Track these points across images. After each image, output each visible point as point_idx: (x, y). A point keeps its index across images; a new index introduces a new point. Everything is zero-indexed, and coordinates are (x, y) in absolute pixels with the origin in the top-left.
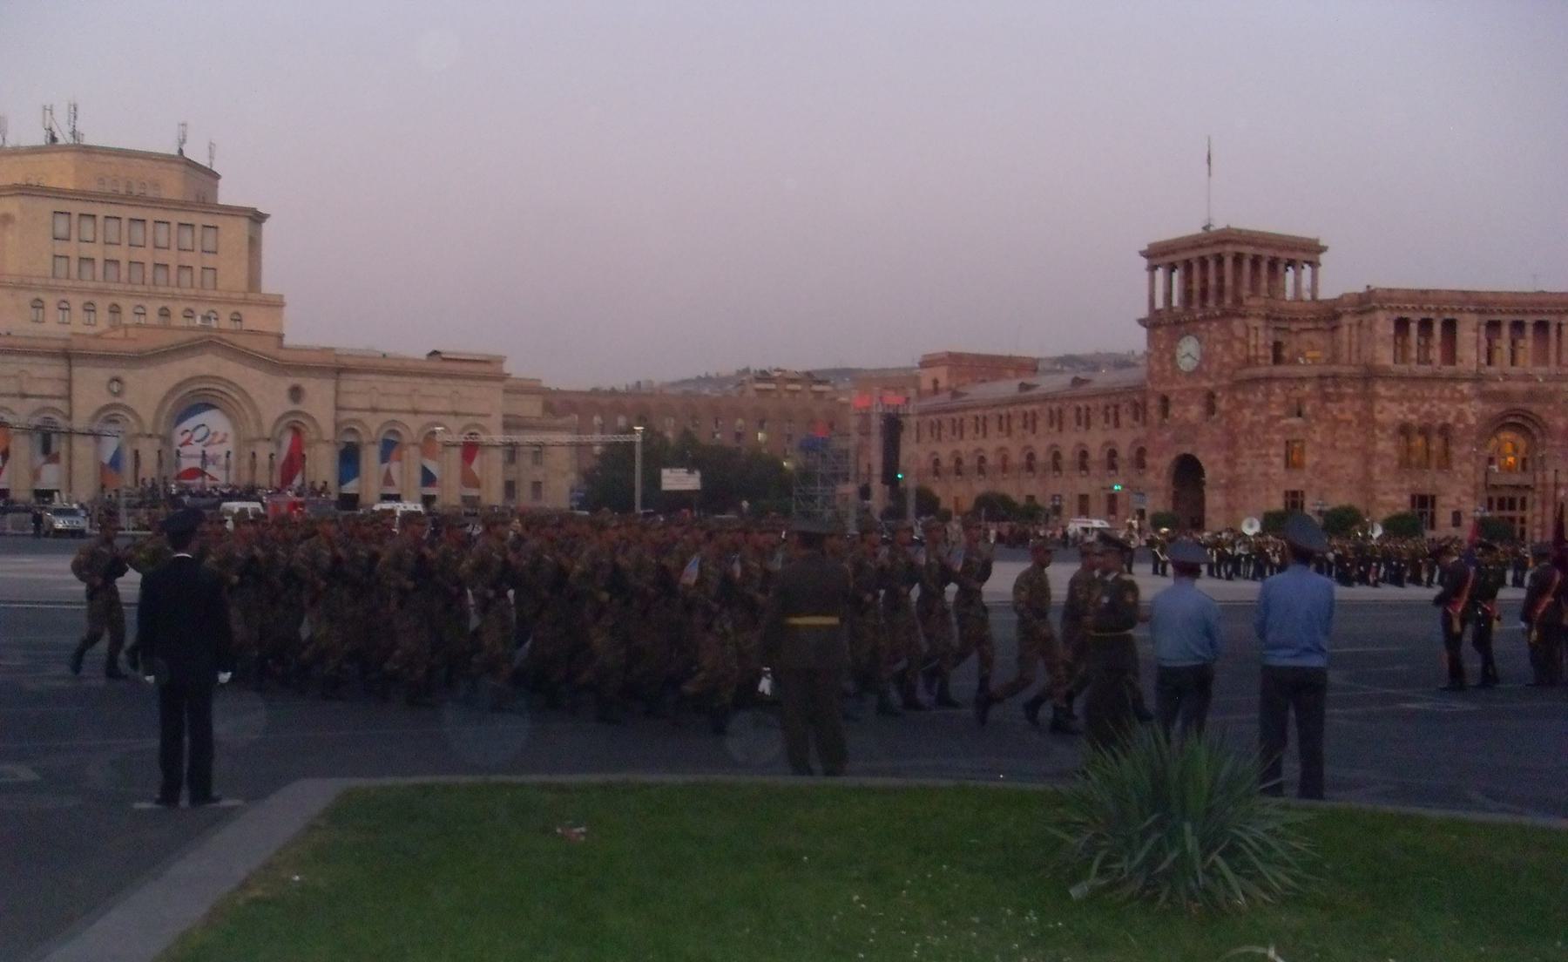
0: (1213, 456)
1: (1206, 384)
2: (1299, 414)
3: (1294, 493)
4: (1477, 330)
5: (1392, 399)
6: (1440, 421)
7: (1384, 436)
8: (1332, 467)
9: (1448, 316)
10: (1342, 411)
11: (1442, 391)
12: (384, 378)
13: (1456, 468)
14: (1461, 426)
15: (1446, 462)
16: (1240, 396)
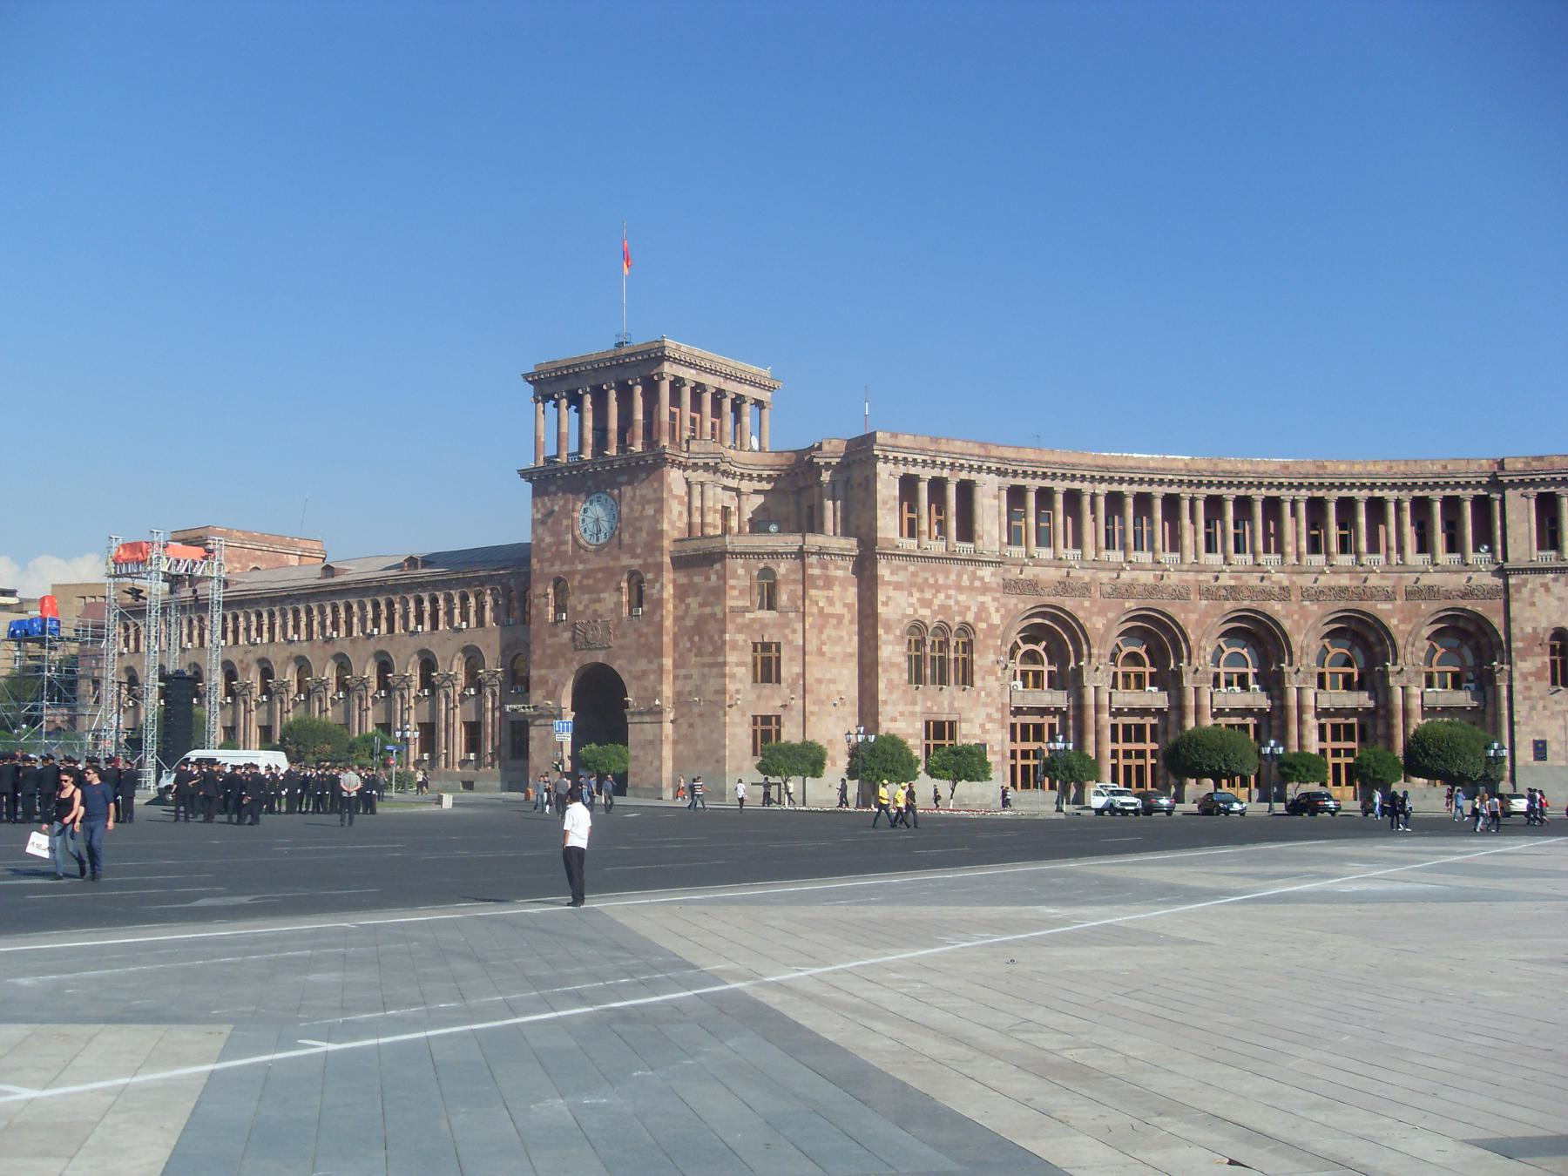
0: (642, 664)
1: (626, 561)
2: (771, 607)
3: (766, 720)
4: (998, 497)
5: (898, 587)
6: (958, 619)
7: (891, 637)
8: (819, 681)
9: (964, 475)
10: (831, 601)
11: (959, 576)
13: (978, 681)
14: (983, 626)
15: (966, 679)
16: (682, 580)
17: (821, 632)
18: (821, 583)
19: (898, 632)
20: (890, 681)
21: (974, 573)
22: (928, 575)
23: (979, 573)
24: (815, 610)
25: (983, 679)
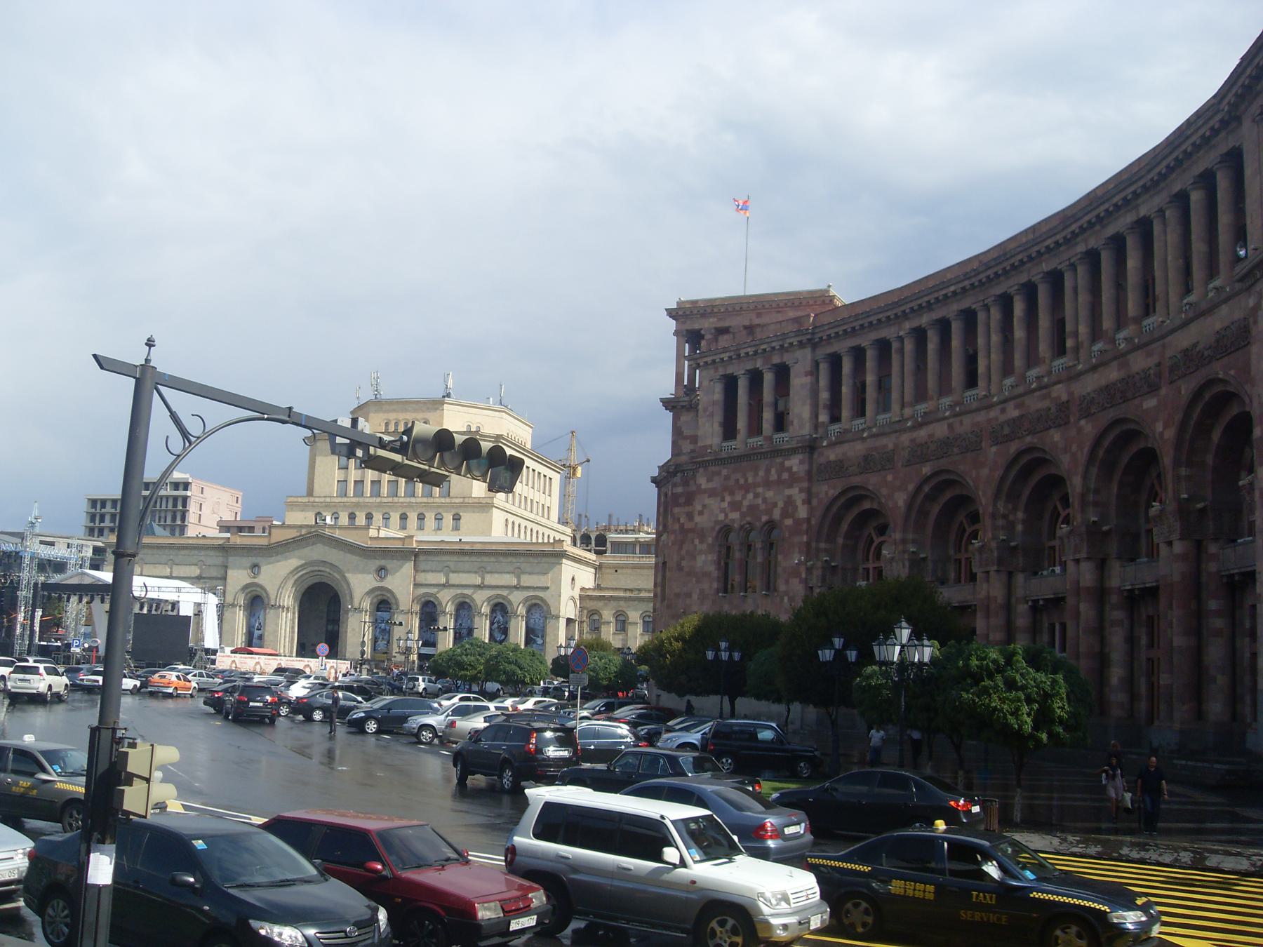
5: (712, 493)
6: (764, 518)
7: (704, 547)
8: (678, 595)
9: (776, 360)
11: (768, 471)
12: (455, 558)
13: (782, 587)
14: (789, 522)
17: (681, 548)
18: (682, 500)
19: (710, 540)
20: (702, 591)
21: (782, 464)
22: (738, 476)
23: (787, 463)
24: (677, 527)
25: (787, 582)
